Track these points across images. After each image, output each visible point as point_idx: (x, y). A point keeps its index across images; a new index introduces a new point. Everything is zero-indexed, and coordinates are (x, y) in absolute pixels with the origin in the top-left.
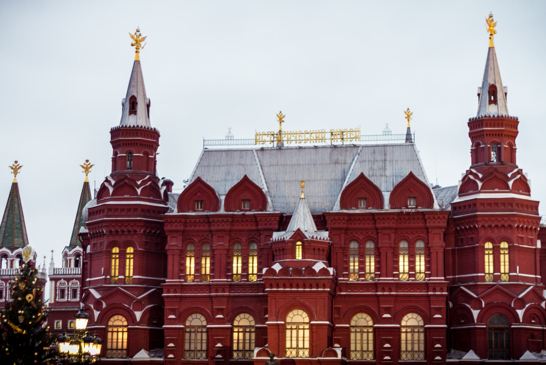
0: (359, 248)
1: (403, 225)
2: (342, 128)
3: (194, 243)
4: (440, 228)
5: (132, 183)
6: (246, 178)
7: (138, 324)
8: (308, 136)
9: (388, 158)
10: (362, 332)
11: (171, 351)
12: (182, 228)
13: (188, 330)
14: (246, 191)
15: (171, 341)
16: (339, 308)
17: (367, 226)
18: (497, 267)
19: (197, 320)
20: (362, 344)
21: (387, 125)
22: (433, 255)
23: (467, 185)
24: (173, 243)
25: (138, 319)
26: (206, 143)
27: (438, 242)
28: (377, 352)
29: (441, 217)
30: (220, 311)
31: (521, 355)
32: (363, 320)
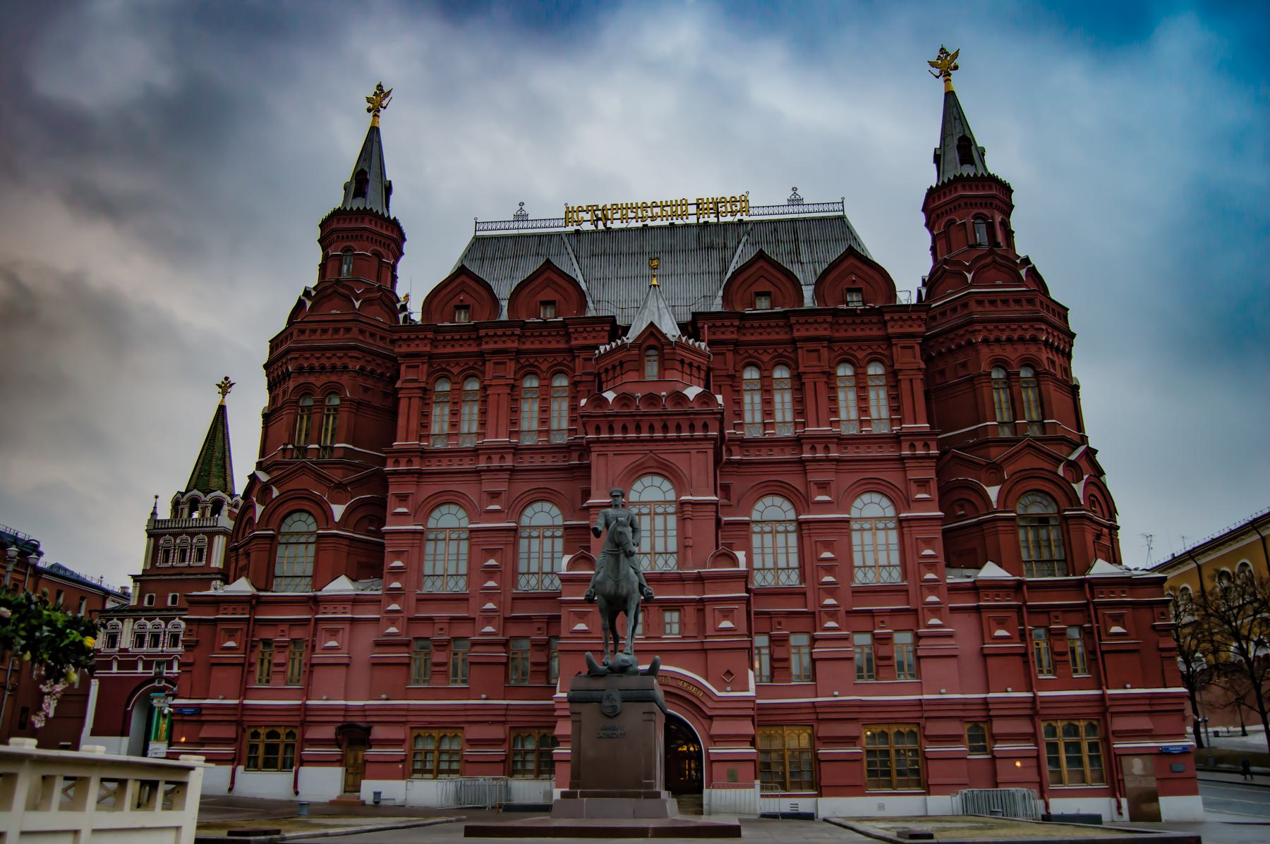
0: (762, 378)
1: (842, 334)
2: (717, 195)
3: (448, 378)
4: (911, 336)
8: (656, 210)
9: (801, 238)
10: (774, 533)
11: (397, 573)
13: (432, 536)
15: (398, 555)
17: (774, 337)
19: (450, 518)
20: (775, 554)
21: (794, 189)
25: (337, 518)
27: (910, 360)
28: (808, 568)
30: (495, 496)
32: (773, 508)
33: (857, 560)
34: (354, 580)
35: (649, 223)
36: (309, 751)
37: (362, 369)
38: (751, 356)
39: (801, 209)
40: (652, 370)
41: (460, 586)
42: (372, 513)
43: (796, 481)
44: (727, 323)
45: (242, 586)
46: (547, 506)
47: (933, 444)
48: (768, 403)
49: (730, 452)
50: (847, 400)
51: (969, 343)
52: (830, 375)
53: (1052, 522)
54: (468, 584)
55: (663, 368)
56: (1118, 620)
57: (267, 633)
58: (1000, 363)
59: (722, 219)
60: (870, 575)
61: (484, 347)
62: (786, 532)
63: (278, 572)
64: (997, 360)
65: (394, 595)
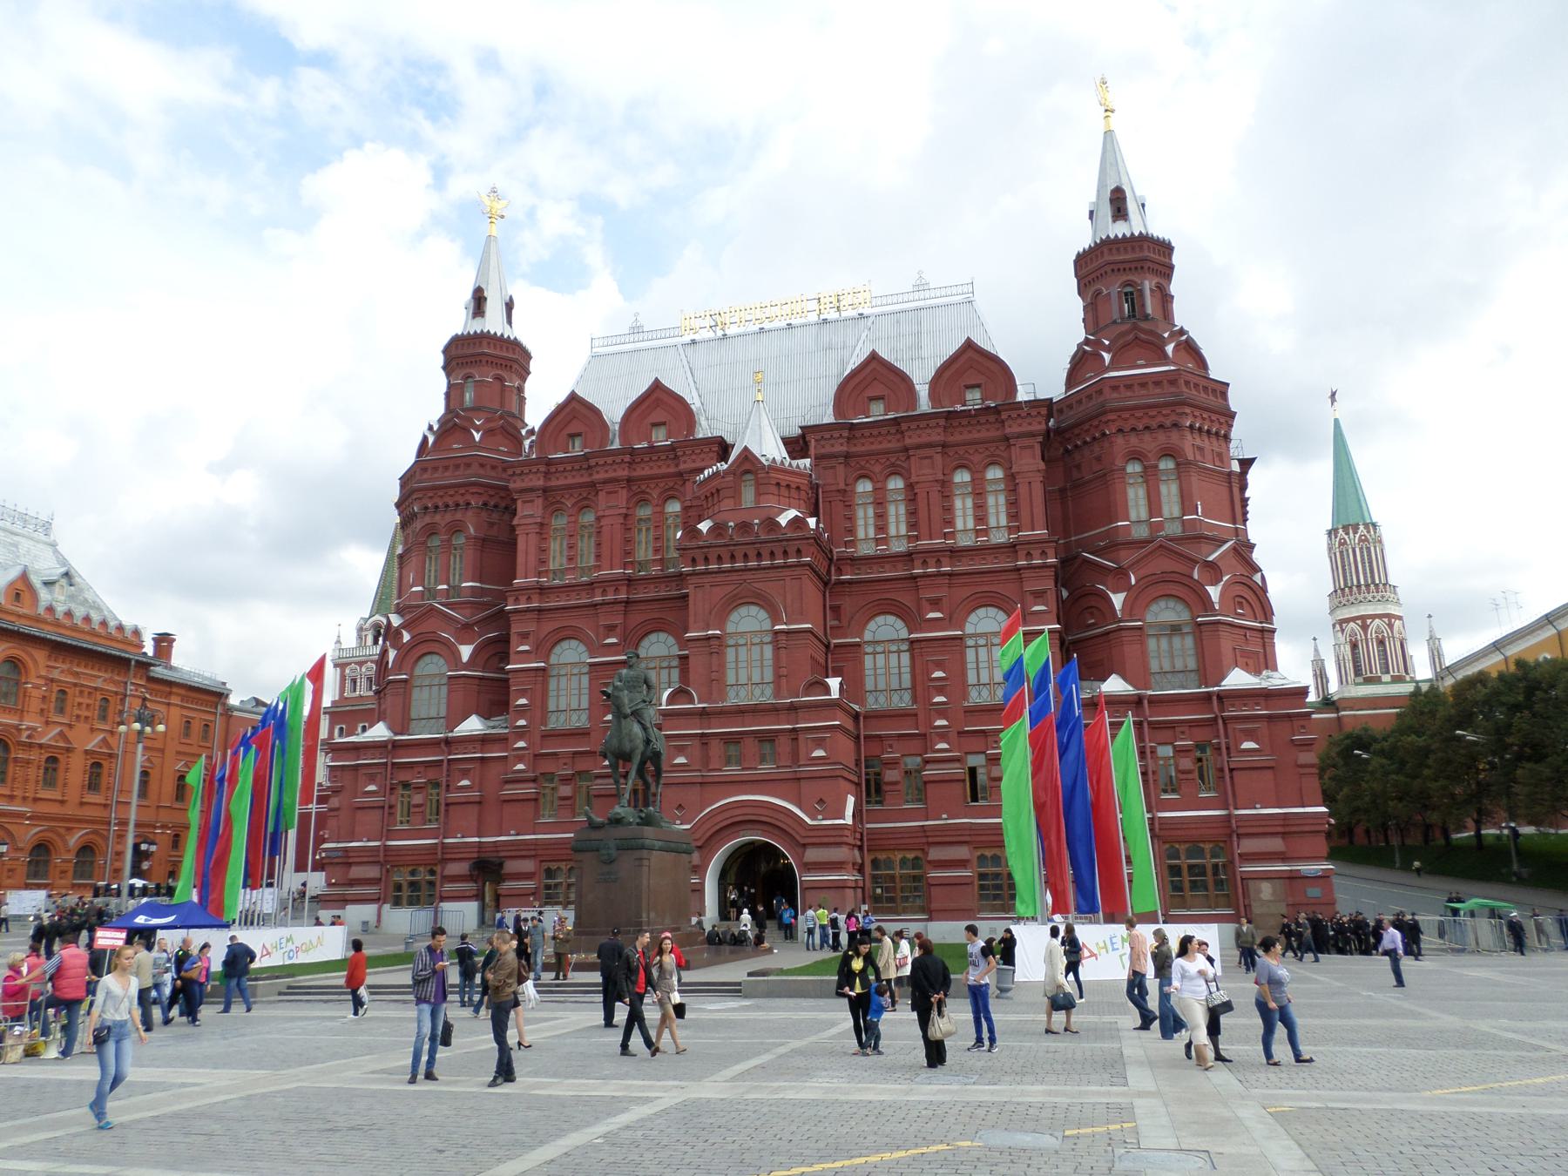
0: (875, 489)
1: (957, 438)
4: (1033, 435)
5: (466, 424)
6: (657, 386)
7: (467, 666)
10: (887, 653)
11: (522, 711)
12: (541, 483)
14: (659, 403)
15: (523, 693)
16: (839, 607)
17: (885, 446)
18: (1154, 506)
19: (571, 653)
22: (1023, 490)
23: (1081, 362)
24: (529, 512)
25: (465, 658)
26: (596, 343)
28: (919, 688)
29: (1034, 413)
30: (610, 629)
31: (1223, 678)
32: (887, 627)
33: (972, 678)
34: (486, 715)
35: (767, 326)
36: (448, 887)
37: (485, 504)
38: (862, 468)
39: (927, 294)
40: (748, 496)
41: (580, 721)
42: (496, 650)
43: (907, 599)
44: (836, 434)
45: (379, 732)
46: (662, 636)
47: (1051, 552)
48: (881, 517)
49: (840, 571)
50: (963, 507)
51: (1104, 434)
52: (945, 486)
53: (1185, 630)
54: (590, 718)
55: (758, 494)
56: (1250, 735)
57: (404, 776)
58: (1136, 456)
59: (844, 314)
60: (985, 693)
61: (596, 477)
62: (899, 652)
63: (413, 715)
64: (1134, 452)
65: (521, 733)
